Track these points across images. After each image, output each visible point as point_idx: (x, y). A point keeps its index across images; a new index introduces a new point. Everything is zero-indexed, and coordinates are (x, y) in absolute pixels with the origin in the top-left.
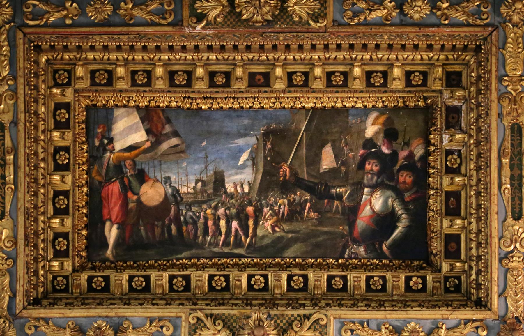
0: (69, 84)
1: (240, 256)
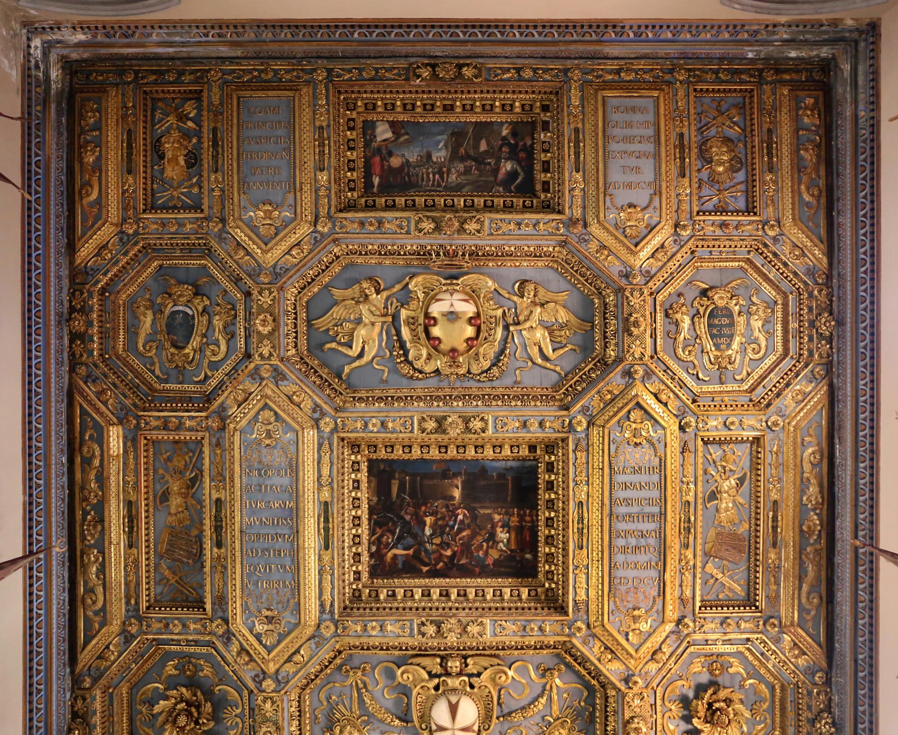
1: (440, 192)
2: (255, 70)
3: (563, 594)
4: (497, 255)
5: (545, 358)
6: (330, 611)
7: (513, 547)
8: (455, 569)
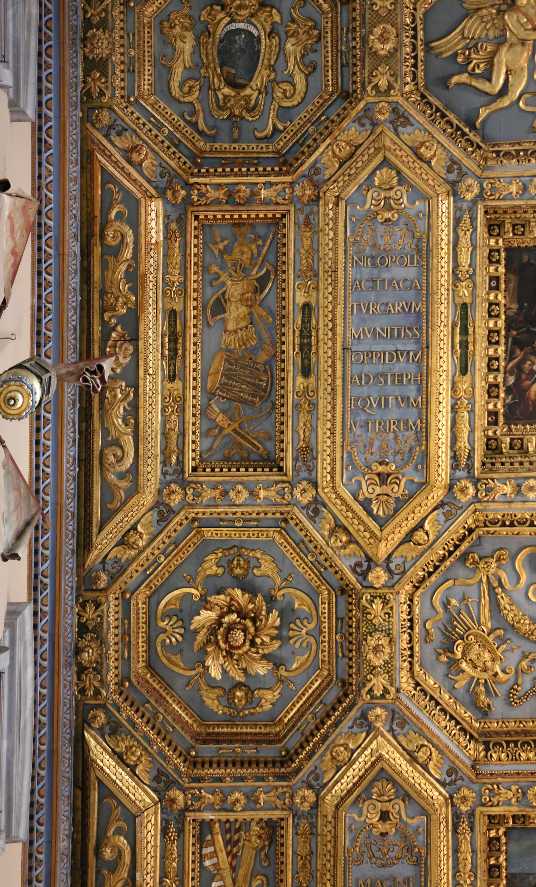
6: (467, 466)
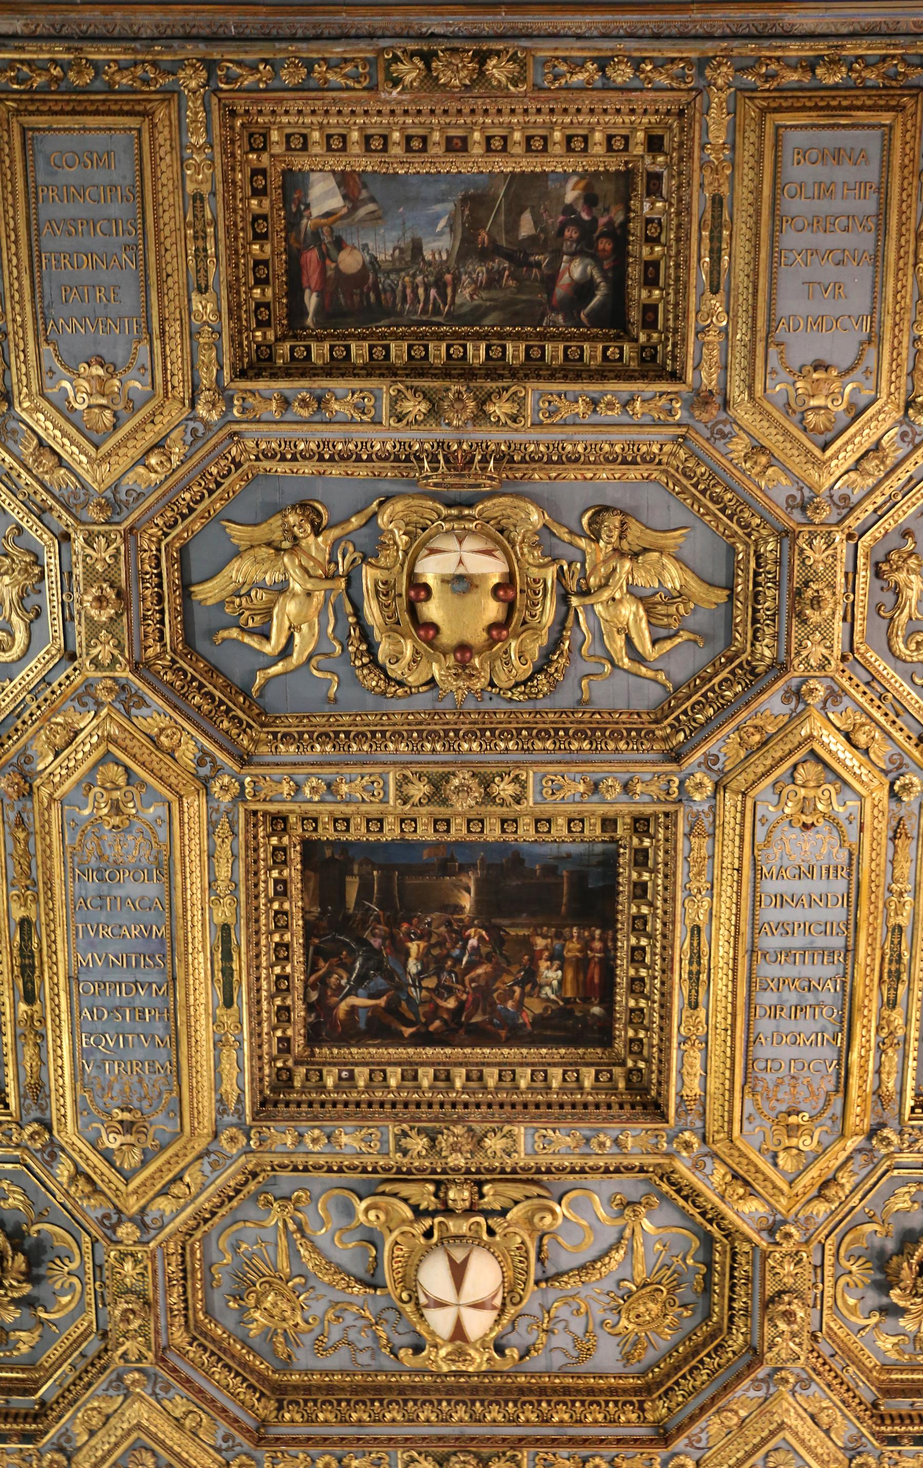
0: (264, 149)
2: (54, 62)
3: (659, 1083)
4: (550, 461)
5: (637, 657)
7: (569, 994)
8: (462, 1032)
